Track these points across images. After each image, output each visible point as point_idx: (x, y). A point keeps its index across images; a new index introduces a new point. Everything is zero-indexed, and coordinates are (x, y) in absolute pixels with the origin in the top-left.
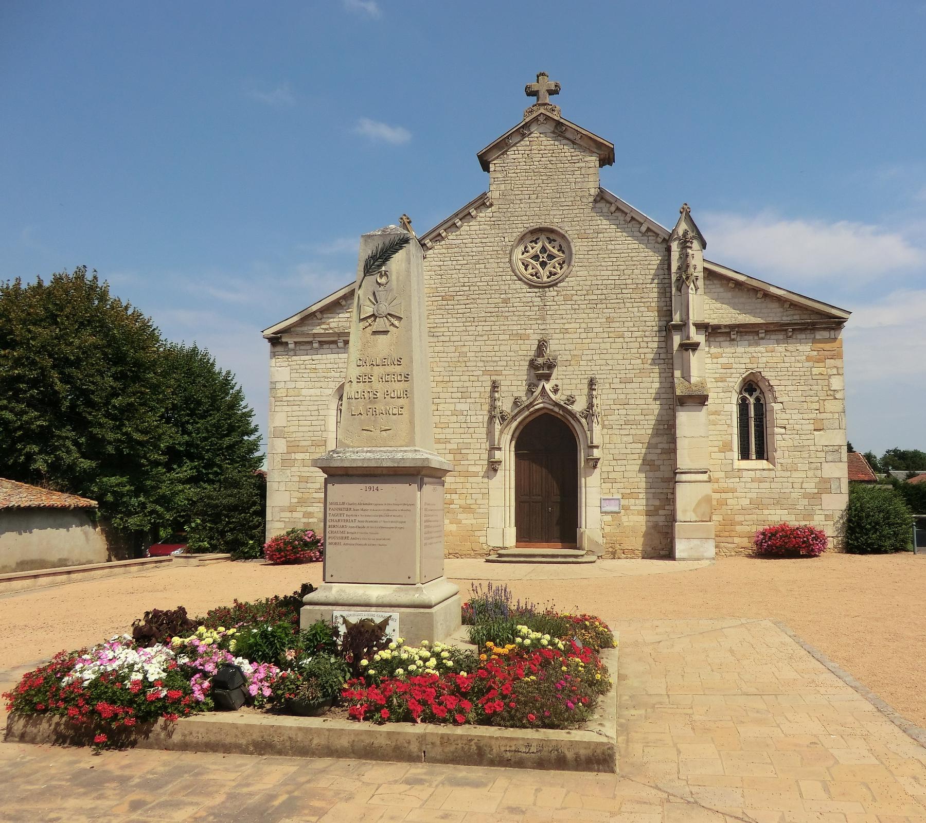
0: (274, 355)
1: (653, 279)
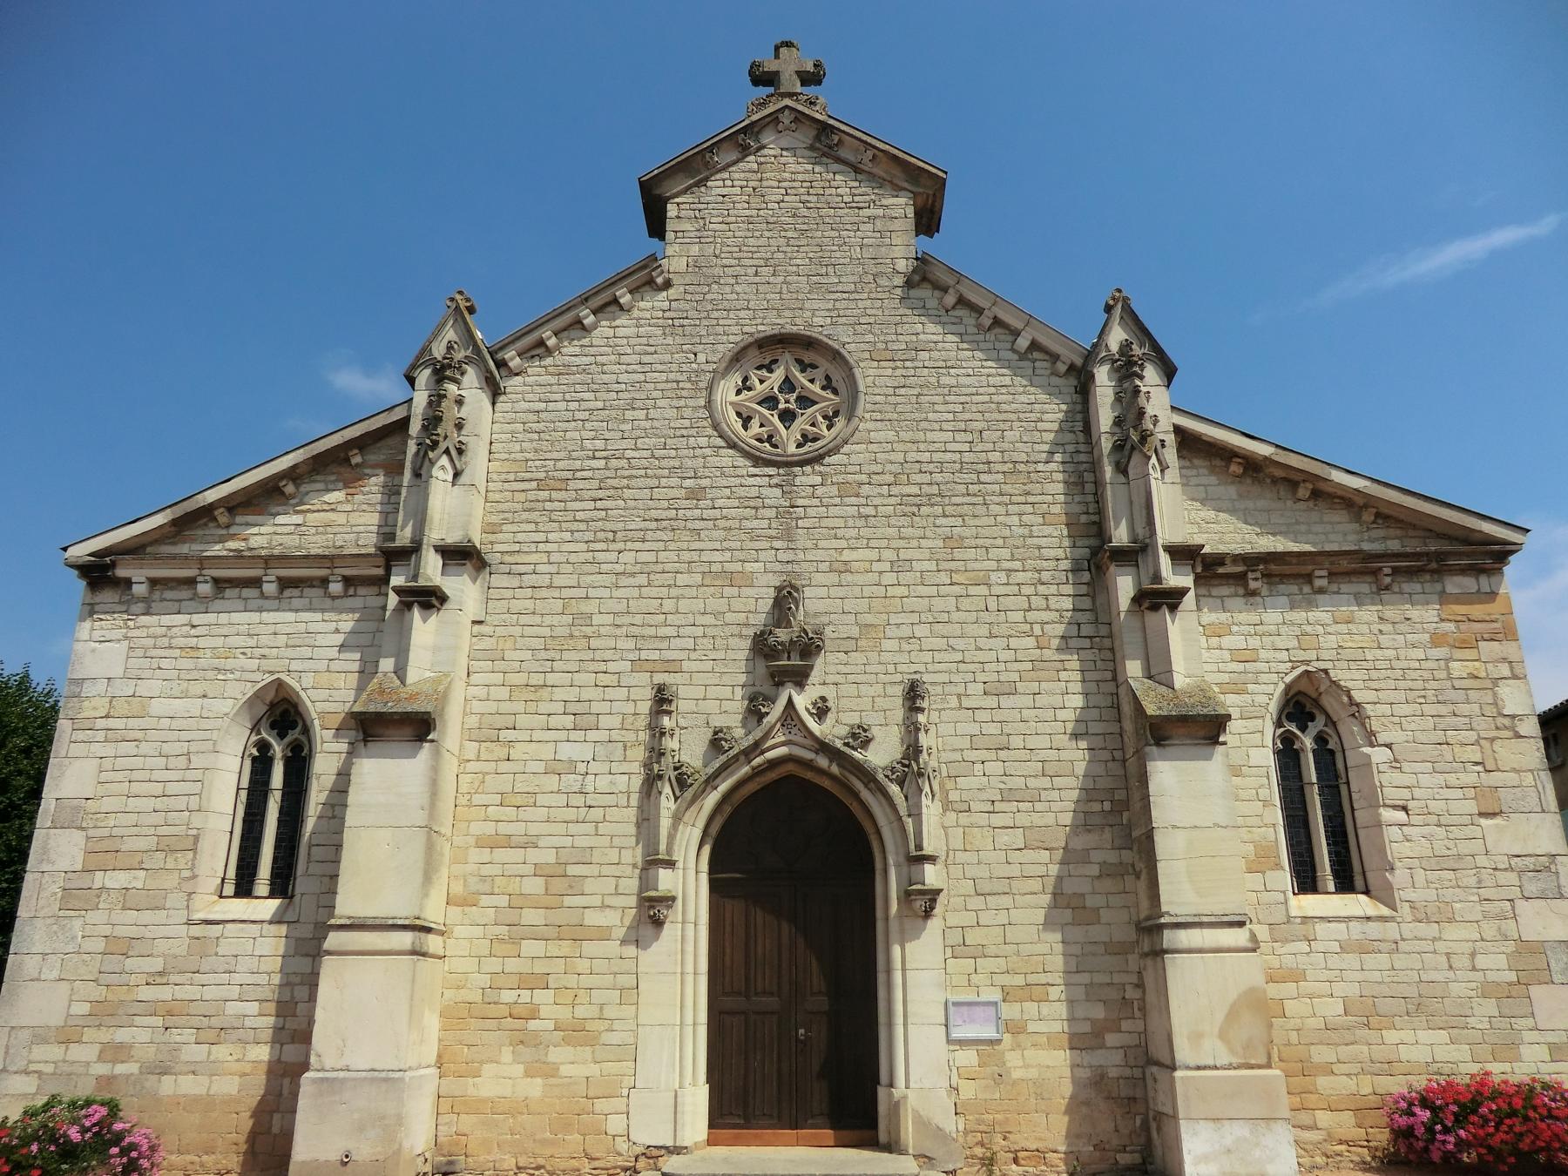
0: (91, 611)
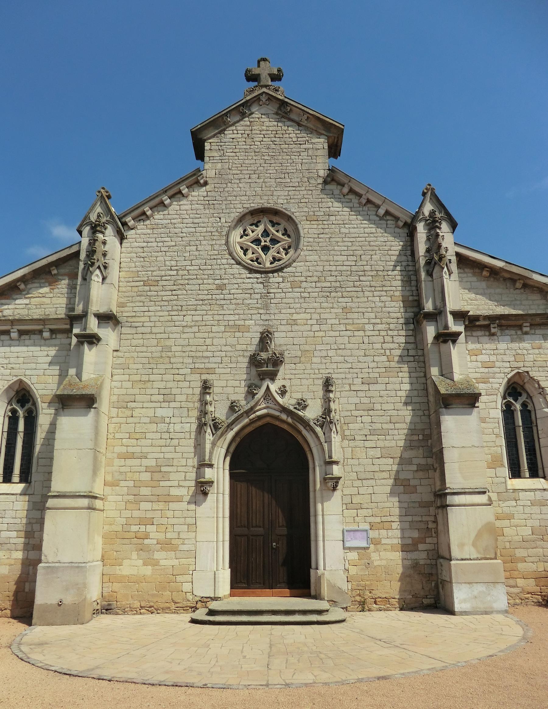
1: (395, 266)
